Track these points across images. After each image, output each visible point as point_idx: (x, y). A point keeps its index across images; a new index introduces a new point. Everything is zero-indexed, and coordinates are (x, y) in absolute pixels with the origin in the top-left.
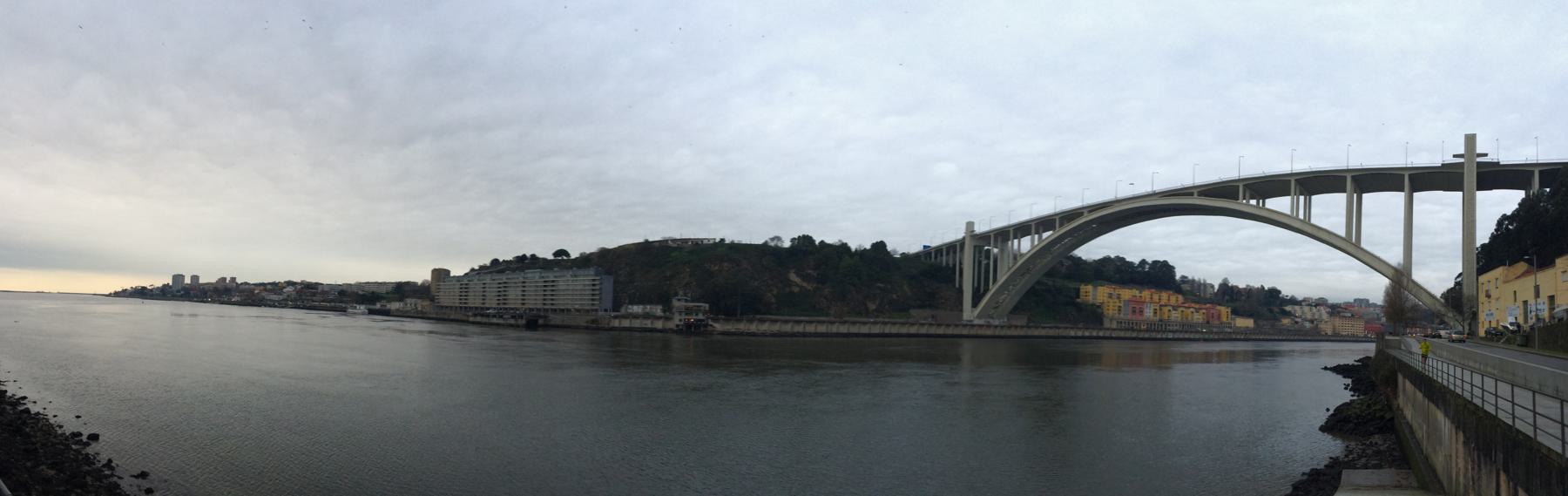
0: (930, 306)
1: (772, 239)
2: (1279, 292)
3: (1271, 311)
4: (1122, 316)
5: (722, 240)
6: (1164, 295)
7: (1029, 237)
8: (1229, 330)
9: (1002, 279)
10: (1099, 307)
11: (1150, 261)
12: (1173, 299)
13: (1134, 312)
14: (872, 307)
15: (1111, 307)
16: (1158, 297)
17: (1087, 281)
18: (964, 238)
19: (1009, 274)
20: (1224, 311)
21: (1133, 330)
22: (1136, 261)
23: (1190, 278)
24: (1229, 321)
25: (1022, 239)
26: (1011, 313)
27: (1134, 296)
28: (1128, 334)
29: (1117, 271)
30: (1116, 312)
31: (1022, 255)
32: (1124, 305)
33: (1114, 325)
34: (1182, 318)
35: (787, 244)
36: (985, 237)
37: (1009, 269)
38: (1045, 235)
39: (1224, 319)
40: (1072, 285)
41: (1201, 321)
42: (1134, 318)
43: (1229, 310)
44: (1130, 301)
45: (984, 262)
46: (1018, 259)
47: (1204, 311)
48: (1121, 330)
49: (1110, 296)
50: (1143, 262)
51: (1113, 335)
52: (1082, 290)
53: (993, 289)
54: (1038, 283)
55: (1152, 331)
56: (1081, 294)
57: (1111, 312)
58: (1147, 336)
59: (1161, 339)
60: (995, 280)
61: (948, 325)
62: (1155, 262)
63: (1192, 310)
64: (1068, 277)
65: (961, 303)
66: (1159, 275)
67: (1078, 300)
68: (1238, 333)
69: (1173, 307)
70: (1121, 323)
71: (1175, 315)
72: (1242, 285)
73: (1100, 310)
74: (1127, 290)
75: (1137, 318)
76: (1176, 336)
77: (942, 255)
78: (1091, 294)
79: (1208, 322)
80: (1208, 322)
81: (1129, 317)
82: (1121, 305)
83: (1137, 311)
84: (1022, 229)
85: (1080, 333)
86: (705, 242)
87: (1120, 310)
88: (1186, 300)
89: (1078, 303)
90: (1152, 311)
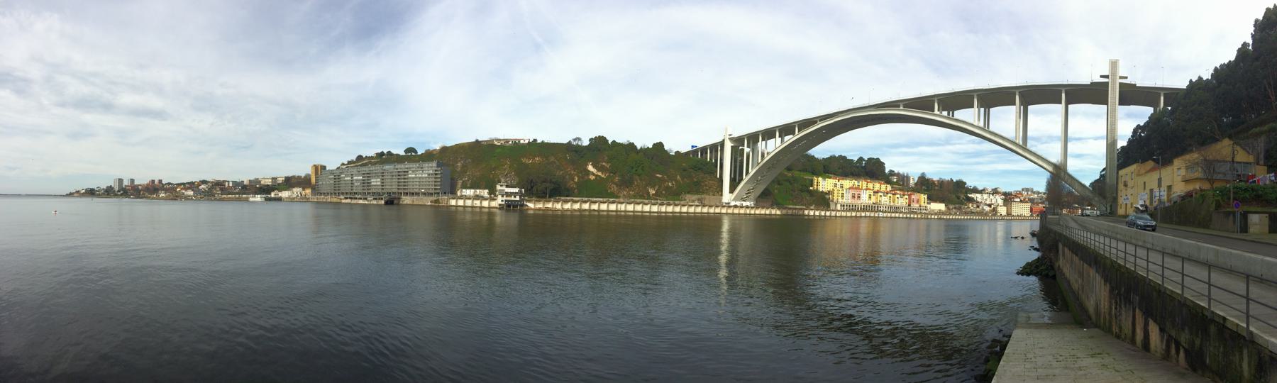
0: (697, 192)
1: (575, 140)
2: (965, 183)
3: (958, 198)
5: (535, 140)
7: (774, 139)
8: (925, 211)
9: (752, 172)
10: (826, 193)
13: (854, 197)
14: (652, 192)
17: (818, 176)
18: (724, 140)
19: (757, 168)
20: (923, 197)
21: (853, 210)
23: (896, 172)
24: (926, 205)
25: (768, 141)
26: (759, 197)
29: (841, 167)
30: (840, 198)
31: (768, 153)
35: (586, 143)
36: (738, 141)
37: (758, 164)
38: (786, 138)
39: (922, 204)
40: (807, 177)
41: (904, 204)
43: (926, 196)
44: (850, 188)
45: (739, 159)
46: (766, 156)
47: (907, 197)
53: (746, 179)
54: (780, 174)
60: (747, 173)
61: (711, 206)
63: (898, 196)
64: (805, 170)
65: (721, 190)
66: (871, 170)
67: (811, 188)
68: (932, 214)
69: (884, 193)
70: (844, 206)
71: (885, 200)
72: (936, 178)
73: (827, 196)
74: (848, 181)
77: (707, 153)
79: (909, 205)
80: (909, 205)
82: (844, 192)
83: (856, 196)
84: (769, 134)
86: (522, 142)
87: (842, 196)
88: (894, 189)
90: (868, 196)
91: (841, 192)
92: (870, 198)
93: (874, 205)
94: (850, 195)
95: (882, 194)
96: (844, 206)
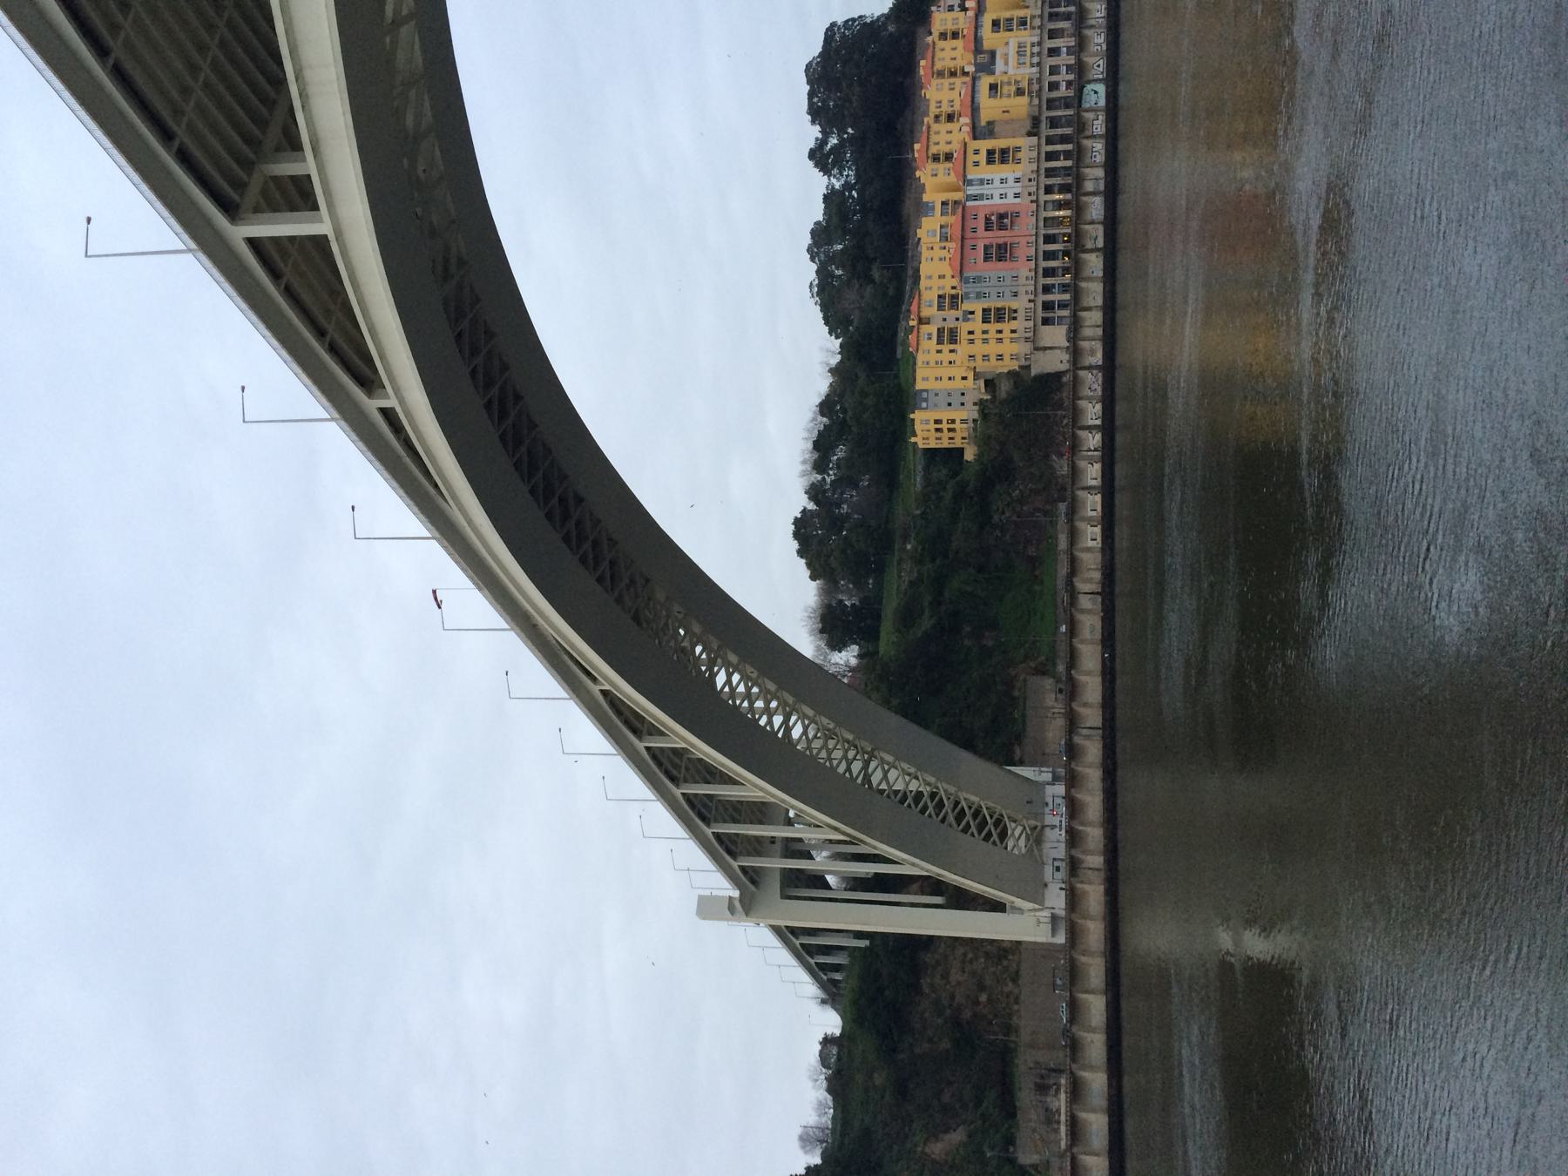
4: (1020, 304)
6: (938, 94)
10: (990, 384)
11: (816, 131)
12: (952, 54)
13: (1001, 253)
15: (993, 348)
16: (943, 127)
21: (1077, 243)
22: (819, 183)
27: (944, 238)
28: (1094, 292)
30: (1006, 327)
32: (979, 296)
33: (1056, 335)
34: (1023, 22)
40: (915, 479)
42: (1025, 250)
48: (1076, 304)
49: (949, 336)
50: (820, 157)
51: (1098, 359)
52: (933, 444)
55: (1080, 179)
56: (945, 444)
57: (1008, 348)
58: (1096, 208)
59: (1112, 138)
62: (816, 113)
67: (969, 455)
70: (1048, 306)
73: (1004, 388)
74: (926, 269)
75: (1025, 234)
76: (1097, 66)
78: (945, 415)
81: (1024, 270)
82: (978, 307)
83: (997, 236)
85: (1092, 473)
87: (1000, 314)
89: (979, 456)
90: (997, 172)
91: (977, 324)
92: (1004, 152)
93: (1045, 131)
94: (994, 270)
95: (985, 82)
96: (1048, 306)
